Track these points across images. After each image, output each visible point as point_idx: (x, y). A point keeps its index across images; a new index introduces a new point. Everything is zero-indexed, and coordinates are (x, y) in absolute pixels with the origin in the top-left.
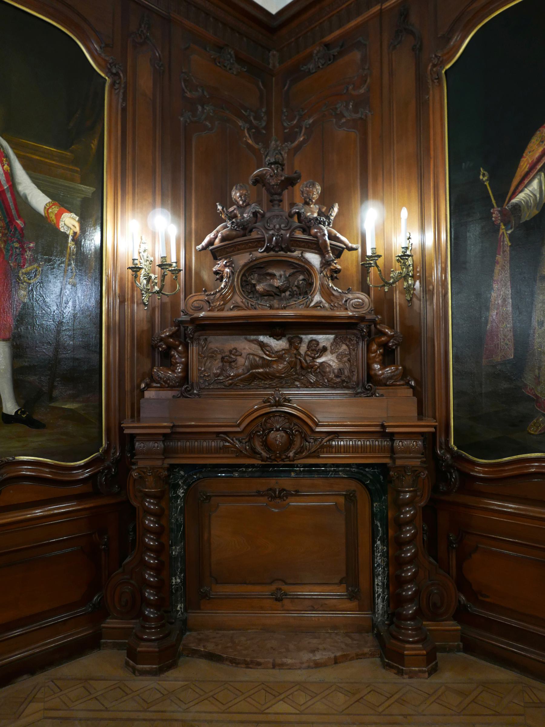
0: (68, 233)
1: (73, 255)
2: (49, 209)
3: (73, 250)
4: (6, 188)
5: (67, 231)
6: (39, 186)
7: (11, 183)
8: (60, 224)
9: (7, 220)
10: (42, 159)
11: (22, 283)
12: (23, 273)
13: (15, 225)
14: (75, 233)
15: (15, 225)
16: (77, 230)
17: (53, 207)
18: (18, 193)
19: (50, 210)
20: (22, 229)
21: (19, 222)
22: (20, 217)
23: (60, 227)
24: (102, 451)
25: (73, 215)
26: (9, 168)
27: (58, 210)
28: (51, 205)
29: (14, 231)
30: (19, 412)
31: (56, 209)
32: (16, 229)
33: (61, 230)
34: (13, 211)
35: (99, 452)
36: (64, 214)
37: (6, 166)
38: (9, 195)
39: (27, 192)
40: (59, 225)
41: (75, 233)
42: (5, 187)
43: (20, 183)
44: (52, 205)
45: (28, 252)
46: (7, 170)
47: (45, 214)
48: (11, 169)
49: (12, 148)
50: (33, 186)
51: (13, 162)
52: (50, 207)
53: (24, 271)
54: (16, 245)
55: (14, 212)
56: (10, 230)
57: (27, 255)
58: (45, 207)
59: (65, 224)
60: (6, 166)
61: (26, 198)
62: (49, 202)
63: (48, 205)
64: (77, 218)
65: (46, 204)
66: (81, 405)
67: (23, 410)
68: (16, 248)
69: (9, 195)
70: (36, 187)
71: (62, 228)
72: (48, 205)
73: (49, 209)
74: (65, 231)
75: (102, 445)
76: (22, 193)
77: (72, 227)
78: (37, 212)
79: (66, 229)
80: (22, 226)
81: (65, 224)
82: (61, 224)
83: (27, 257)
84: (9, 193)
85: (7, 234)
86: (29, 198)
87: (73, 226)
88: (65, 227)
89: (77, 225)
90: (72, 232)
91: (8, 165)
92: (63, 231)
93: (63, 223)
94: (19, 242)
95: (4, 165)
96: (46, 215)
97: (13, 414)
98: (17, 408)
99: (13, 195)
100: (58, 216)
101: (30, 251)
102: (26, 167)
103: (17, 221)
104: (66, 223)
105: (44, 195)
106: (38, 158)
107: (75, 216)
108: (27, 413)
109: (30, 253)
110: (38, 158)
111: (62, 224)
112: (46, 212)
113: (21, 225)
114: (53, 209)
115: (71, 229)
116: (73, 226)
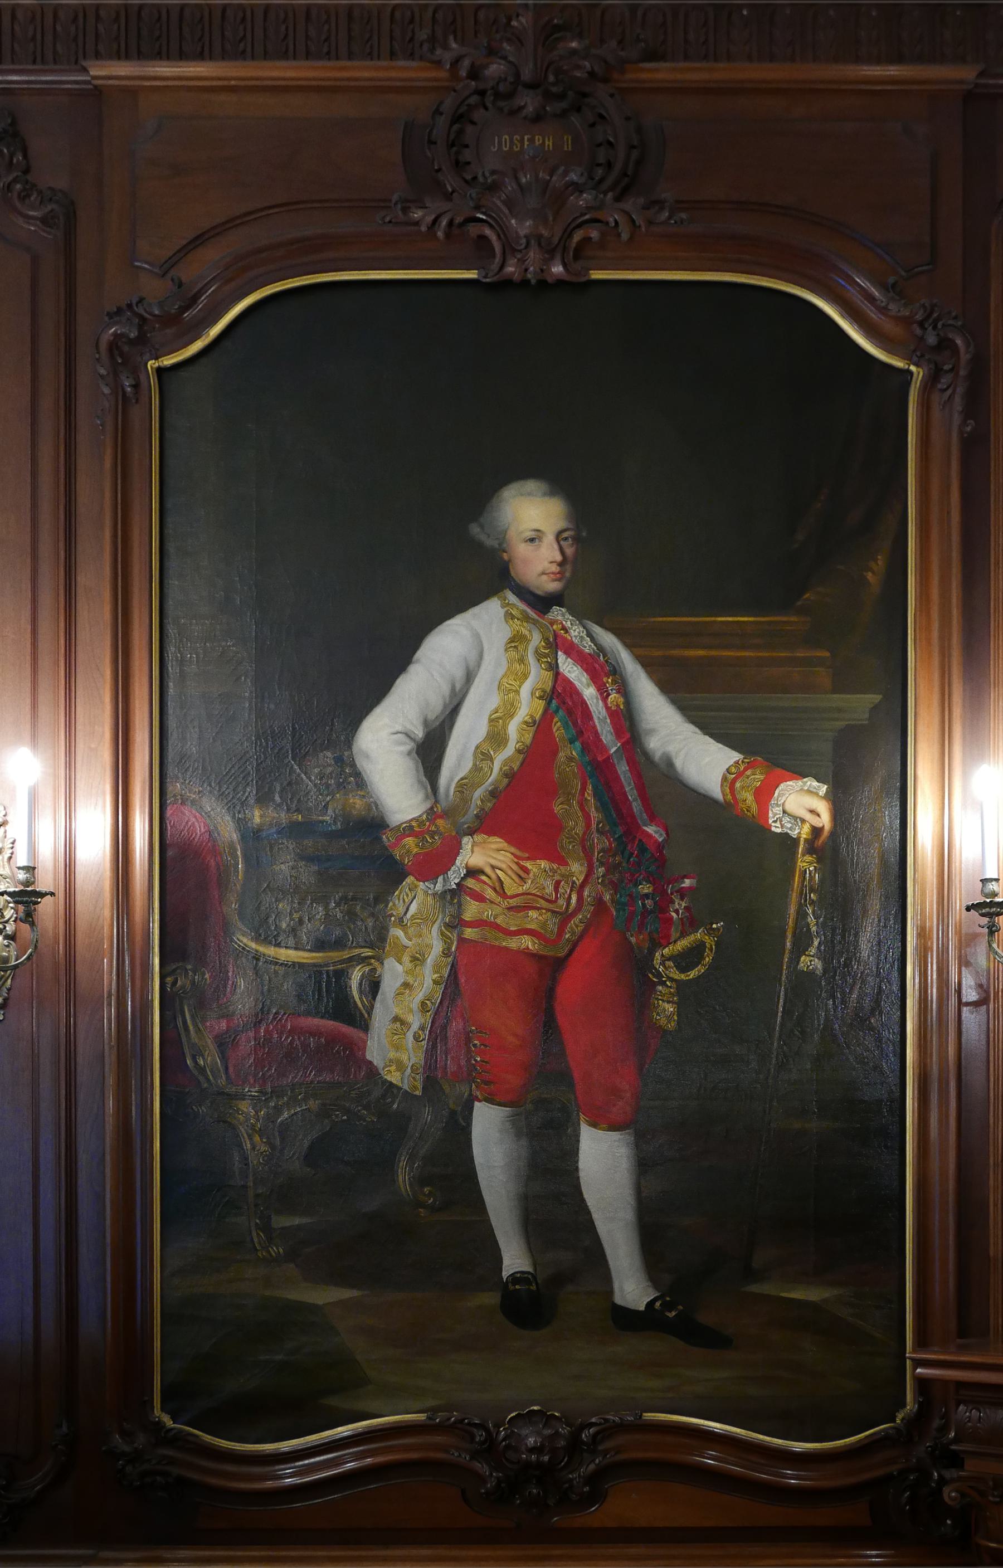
0: (794, 834)
1: (812, 890)
2: (734, 781)
3: (811, 878)
4: (615, 752)
5: (791, 829)
6: (707, 728)
7: (628, 735)
8: (770, 815)
9: (619, 831)
10: (713, 653)
11: (664, 983)
12: (665, 959)
13: (640, 841)
14: (816, 831)
15: (640, 841)
16: (825, 820)
17: (748, 772)
18: (646, 755)
19: (738, 785)
20: (660, 847)
21: (651, 829)
22: (652, 818)
23: (770, 821)
24: (903, 1419)
25: (811, 783)
26: (621, 700)
27: (762, 777)
28: (742, 769)
29: (637, 856)
30: (658, 1304)
31: (757, 777)
32: (643, 850)
33: (773, 829)
34: (634, 804)
35: (894, 1421)
36: (782, 786)
37: (613, 696)
38: (622, 768)
39: (671, 749)
40: (767, 818)
41: (816, 831)
42: (613, 750)
43: (651, 732)
44: (746, 769)
45: (677, 901)
46: (618, 706)
47: (724, 795)
48: (628, 703)
49: (628, 646)
50: (689, 730)
51: (631, 681)
52: (740, 775)
53: (666, 951)
54: (646, 888)
55: (637, 806)
56: (627, 853)
57: (677, 911)
58: (724, 779)
59: (784, 812)
60: (613, 696)
61: (670, 763)
62: (737, 762)
63: (733, 770)
64: (824, 789)
65: (727, 770)
66: (835, 1292)
67: (668, 1299)
68: (646, 896)
69: (622, 768)
70: (697, 730)
71: (778, 824)
72: (733, 770)
73: (734, 781)
74: (786, 830)
75: (904, 1405)
76: (657, 757)
77: (808, 817)
78: (700, 794)
79: (789, 825)
80: (660, 840)
81: (784, 812)
82: (774, 813)
83: (674, 915)
84: (624, 762)
85: (620, 864)
86: (678, 763)
87: (812, 811)
88: (786, 819)
89: (823, 808)
90: (806, 829)
91: (618, 692)
92: (779, 830)
93: (778, 810)
94: (650, 879)
95: (609, 695)
96: (729, 797)
97: (642, 1308)
98: (651, 1295)
99: (632, 763)
100: (764, 794)
101: (682, 899)
102: (667, 687)
103: (645, 828)
104: (788, 807)
105: (720, 746)
106: (701, 653)
107: (815, 784)
108: (681, 1307)
109: (684, 904)
110: (701, 653)
111: (775, 814)
112: (728, 790)
113: (656, 836)
114: (748, 777)
115: (803, 821)
116: (812, 811)
